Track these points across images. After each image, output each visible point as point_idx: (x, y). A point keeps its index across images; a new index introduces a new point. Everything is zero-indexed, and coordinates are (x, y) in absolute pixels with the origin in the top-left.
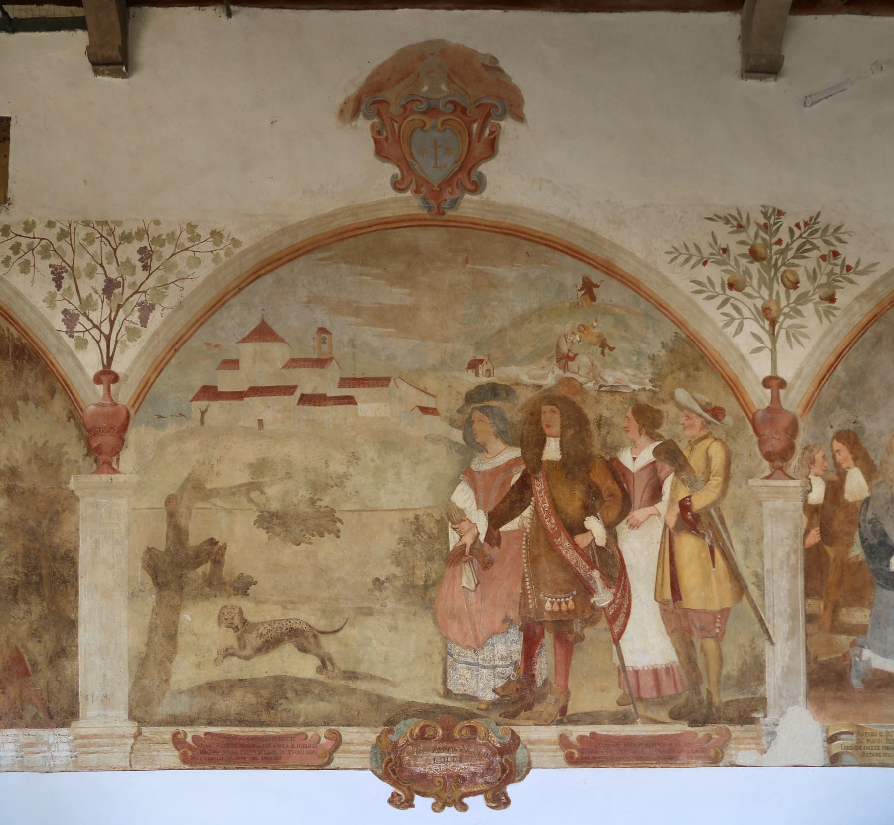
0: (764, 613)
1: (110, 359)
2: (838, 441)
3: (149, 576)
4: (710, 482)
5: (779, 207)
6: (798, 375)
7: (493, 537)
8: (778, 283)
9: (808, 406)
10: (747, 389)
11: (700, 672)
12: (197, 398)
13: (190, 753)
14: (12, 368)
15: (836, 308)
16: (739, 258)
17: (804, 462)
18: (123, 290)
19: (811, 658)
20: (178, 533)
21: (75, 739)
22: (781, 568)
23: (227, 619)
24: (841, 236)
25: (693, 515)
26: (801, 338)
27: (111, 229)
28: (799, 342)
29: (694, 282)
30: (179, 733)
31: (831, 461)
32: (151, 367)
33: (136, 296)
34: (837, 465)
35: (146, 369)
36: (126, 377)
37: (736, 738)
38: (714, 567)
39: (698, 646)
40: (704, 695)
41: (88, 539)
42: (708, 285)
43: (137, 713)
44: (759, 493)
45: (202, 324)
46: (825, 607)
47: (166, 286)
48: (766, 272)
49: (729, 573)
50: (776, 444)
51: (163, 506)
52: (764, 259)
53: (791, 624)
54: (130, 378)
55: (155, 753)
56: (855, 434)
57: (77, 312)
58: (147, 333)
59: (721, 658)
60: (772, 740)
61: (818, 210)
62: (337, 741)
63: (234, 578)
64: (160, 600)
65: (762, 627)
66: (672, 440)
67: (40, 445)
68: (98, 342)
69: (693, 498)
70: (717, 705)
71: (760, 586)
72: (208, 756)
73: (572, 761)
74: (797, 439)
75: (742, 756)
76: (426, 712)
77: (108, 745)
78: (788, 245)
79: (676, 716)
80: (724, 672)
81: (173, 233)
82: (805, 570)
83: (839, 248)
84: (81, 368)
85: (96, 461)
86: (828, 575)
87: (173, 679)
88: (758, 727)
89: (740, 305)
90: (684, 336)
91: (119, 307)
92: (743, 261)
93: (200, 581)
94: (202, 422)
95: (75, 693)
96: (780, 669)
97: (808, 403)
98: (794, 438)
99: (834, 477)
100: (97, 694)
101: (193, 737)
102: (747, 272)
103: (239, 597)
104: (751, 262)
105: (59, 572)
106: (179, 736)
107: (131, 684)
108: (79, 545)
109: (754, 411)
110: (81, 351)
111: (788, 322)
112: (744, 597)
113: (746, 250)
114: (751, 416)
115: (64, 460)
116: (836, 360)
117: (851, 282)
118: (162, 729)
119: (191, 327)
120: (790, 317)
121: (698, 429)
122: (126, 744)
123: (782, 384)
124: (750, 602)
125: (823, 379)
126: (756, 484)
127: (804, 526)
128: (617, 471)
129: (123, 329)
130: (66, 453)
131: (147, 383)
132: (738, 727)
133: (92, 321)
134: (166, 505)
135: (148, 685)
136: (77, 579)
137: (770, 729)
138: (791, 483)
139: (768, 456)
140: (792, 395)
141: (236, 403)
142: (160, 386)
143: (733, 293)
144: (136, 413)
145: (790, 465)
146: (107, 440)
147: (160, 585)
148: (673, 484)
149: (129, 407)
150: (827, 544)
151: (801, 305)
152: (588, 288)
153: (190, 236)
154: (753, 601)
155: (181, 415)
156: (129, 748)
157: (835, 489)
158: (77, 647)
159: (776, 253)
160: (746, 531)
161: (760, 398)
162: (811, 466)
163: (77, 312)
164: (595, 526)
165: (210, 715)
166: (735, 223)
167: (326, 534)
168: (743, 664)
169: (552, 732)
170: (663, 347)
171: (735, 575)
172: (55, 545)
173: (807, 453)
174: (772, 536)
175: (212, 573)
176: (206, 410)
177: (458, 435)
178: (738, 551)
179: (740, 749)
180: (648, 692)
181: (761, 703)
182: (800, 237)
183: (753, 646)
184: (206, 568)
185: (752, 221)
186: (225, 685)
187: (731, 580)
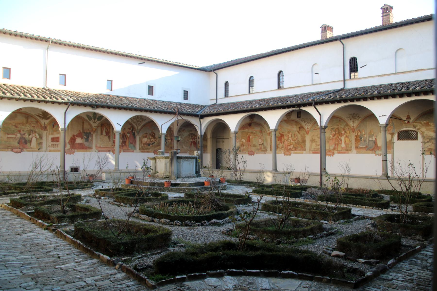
20: (312, 138)
76: (328, 150)
128: (341, 133)
152: (340, 120)
157: (358, 134)
161: (352, 127)
164: (340, 137)
171: (350, 140)
181: (351, 149)
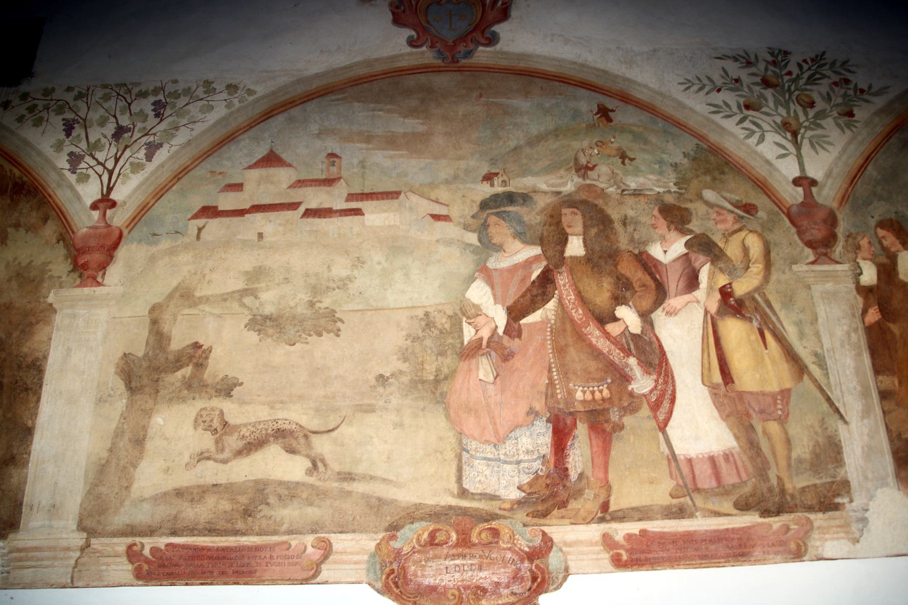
0: (831, 391)
1: (110, 189)
2: (882, 228)
3: (122, 382)
4: (749, 270)
5: (784, 48)
6: (828, 175)
7: (513, 330)
8: (794, 104)
9: (843, 200)
10: (777, 188)
11: (766, 458)
12: (196, 216)
13: (146, 567)
14: (9, 201)
15: (856, 121)
16: (752, 86)
17: (849, 248)
18: (132, 134)
19: (894, 435)
21: (10, 552)
22: (843, 346)
23: (205, 422)
24: (850, 68)
25: (736, 301)
26: (825, 146)
27: (128, 89)
28: (823, 148)
29: (710, 105)
30: (135, 544)
31: (878, 246)
32: (150, 194)
33: (146, 137)
34: (884, 249)
35: (146, 196)
36: (125, 203)
37: (819, 528)
38: (766, 348)
39: (759, 428)
40: (774, 482)
41: (60, 347)
42: (724, 107)
43: (88, 523)
44: (805, 277)
45: (208, 156)
46: (900, 383)
47: (177, 128)
48: (781, 96)
49: (785, 354)
50: (817, 233)
51: (147, 313)
52: (777, 86)
53: (864, 401)
54: (128, 204)
55: (104, 568)
56: (898, 222)
57: (83, 153)
58: (150, 167)
59: (788, 441)
60: (864, 527)
61: (822, 50)
62: (327, 550)
63: (217, 380)
64: (130, 405)
65: (831, 406)
66: (704, 234)
67: (24, 264)
68: (100, 176)
69: (734, 285)
70: (790, 491)
71: (821, 362)
72: (167, 571)
73: (619, 563)
74: (838, 228)
75: (830, 547)
76: (437, 514)
77: (48, 559)
78: (798, 75)
79: (743, 506)
80: (794, 455)
81: (189, 88)
82: (870, 347)
83: (849, 76)
84: (78, 197)
85: (80, 276)
86: (896, 351)
87: (135, 486)
88: (844, 514)
89: (760, 122)
90: (706, 147)
91: (126, 147)
92: (757, 89)
93: (178, 384)
94: (198, 237)
95: (18, 502)
96: (860, 449)
97: (843, 198)
98: (835, 228)
99: (883, 260)
100: (44, 503)
101: (151, 549)
102: (761, 96)
103: (221, 398)
104: (765, 89)
105: (22, 380)
106: (135, 548)
107: (85, 492)
108: (48, 354)
109: (788, 206)
110: (82, 185)
111: (809, 133)
112: (806, 377)
113: (758, 80)
114: (786, 211)
115: (47, 276)
116: (866, 161)
117: (867, 101)
118: (115, 540)
119: (197, 160)
120: (812, 129)
121: (731, 223)
122: (70, 558)
123: (813, 182)
124: (813, 382)
125: (855, 177)
126: (800, 269)
127: (861, 306)
129: (128, 164)
130: (50, 270)
131: (145, 207)
132: (820, 515)
133: (97, 160)
134: (150, 313)
135: (106, 493)
136: (41, 387)
137: (859, 515)
138: (838, 267)
139: (810, 244)
140: (825, 192)
141: (236, 220)
142: (159, 209)
143: (751, 112)
144: (129, 232)
145: (835, 251)
146: (95, 257)
147: (132, 389)
148: (710, 273)
149: (123, 229)
150: (889, 321)
151: (820, 119)
152: (604, 113)
153: (205, 89)
154: (816, 381)
155: (177, 232)
156: (73, 562)
158: (29, 454)
159: (788, 81)
160: (797, 313)
162: (857, 251)
163: (83, 153)
165: (174, 524)
166: (744, 61)
167: (324, 333)
168: (815, 446)
169: (594, 531)
170: (685, 156)
172: (22, 354)
173: (850, 240)
174: (827, 317)
175: (193, 376)
176: (204, 227)
177: (472, 238)
178: (791, 333)
179: (826, 540)
180: (706, 480)
182: (809, 69)
183: (824, 426)
184: (187, 371)
185: (760, 59)
186: (195, 491)
187: (787, 361)
